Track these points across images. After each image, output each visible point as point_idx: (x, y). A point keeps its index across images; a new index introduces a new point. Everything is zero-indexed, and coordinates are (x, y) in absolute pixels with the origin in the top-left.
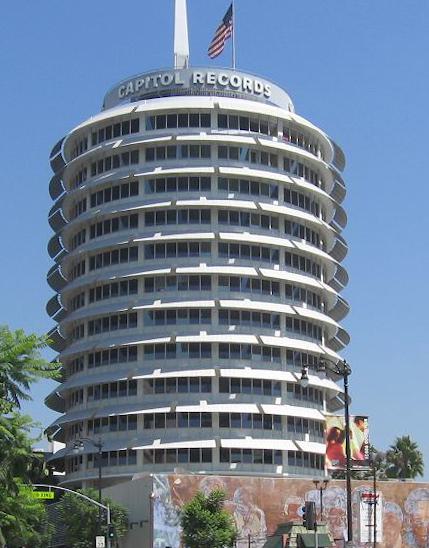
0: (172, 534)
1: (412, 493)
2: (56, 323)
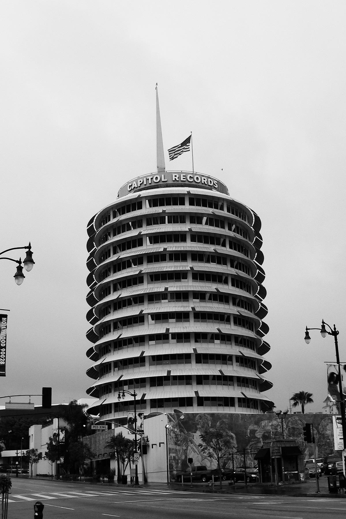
0: (179, 451)
1: (323, 421)
2: (91, 326)
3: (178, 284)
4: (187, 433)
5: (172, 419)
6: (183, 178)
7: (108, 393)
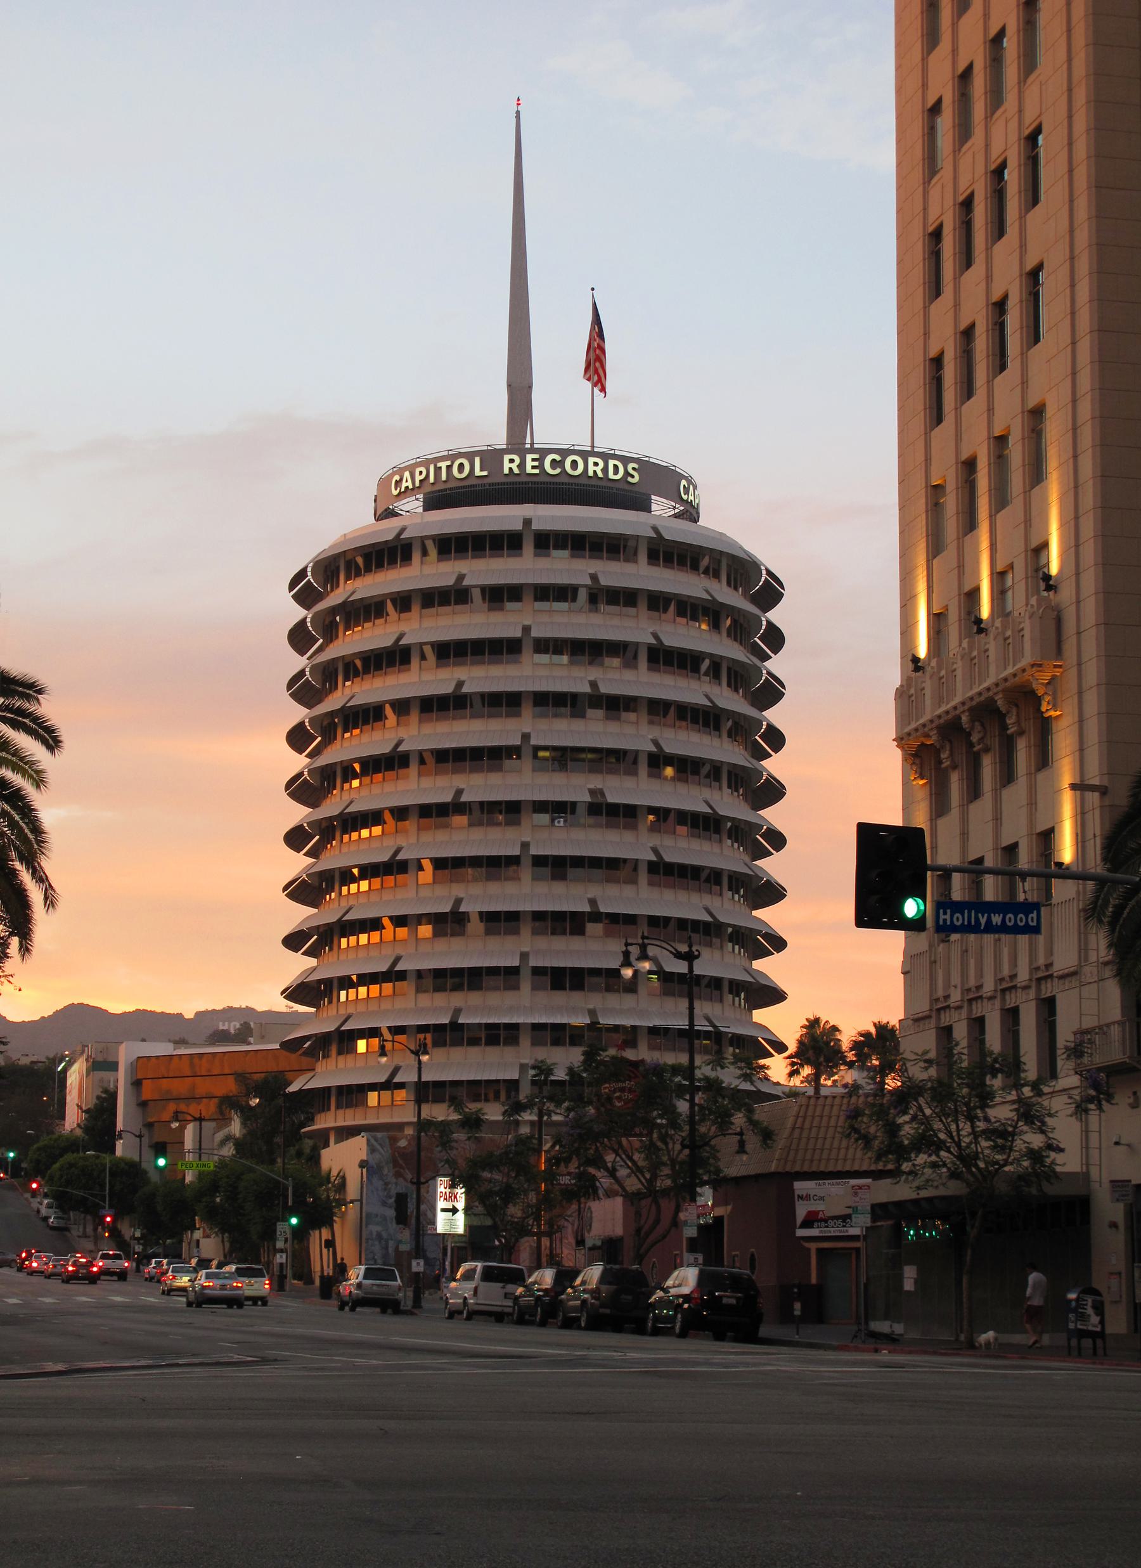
3: (494, 778)
5: (378, 1147)
6: (533, 467)
7: (343, 1054)
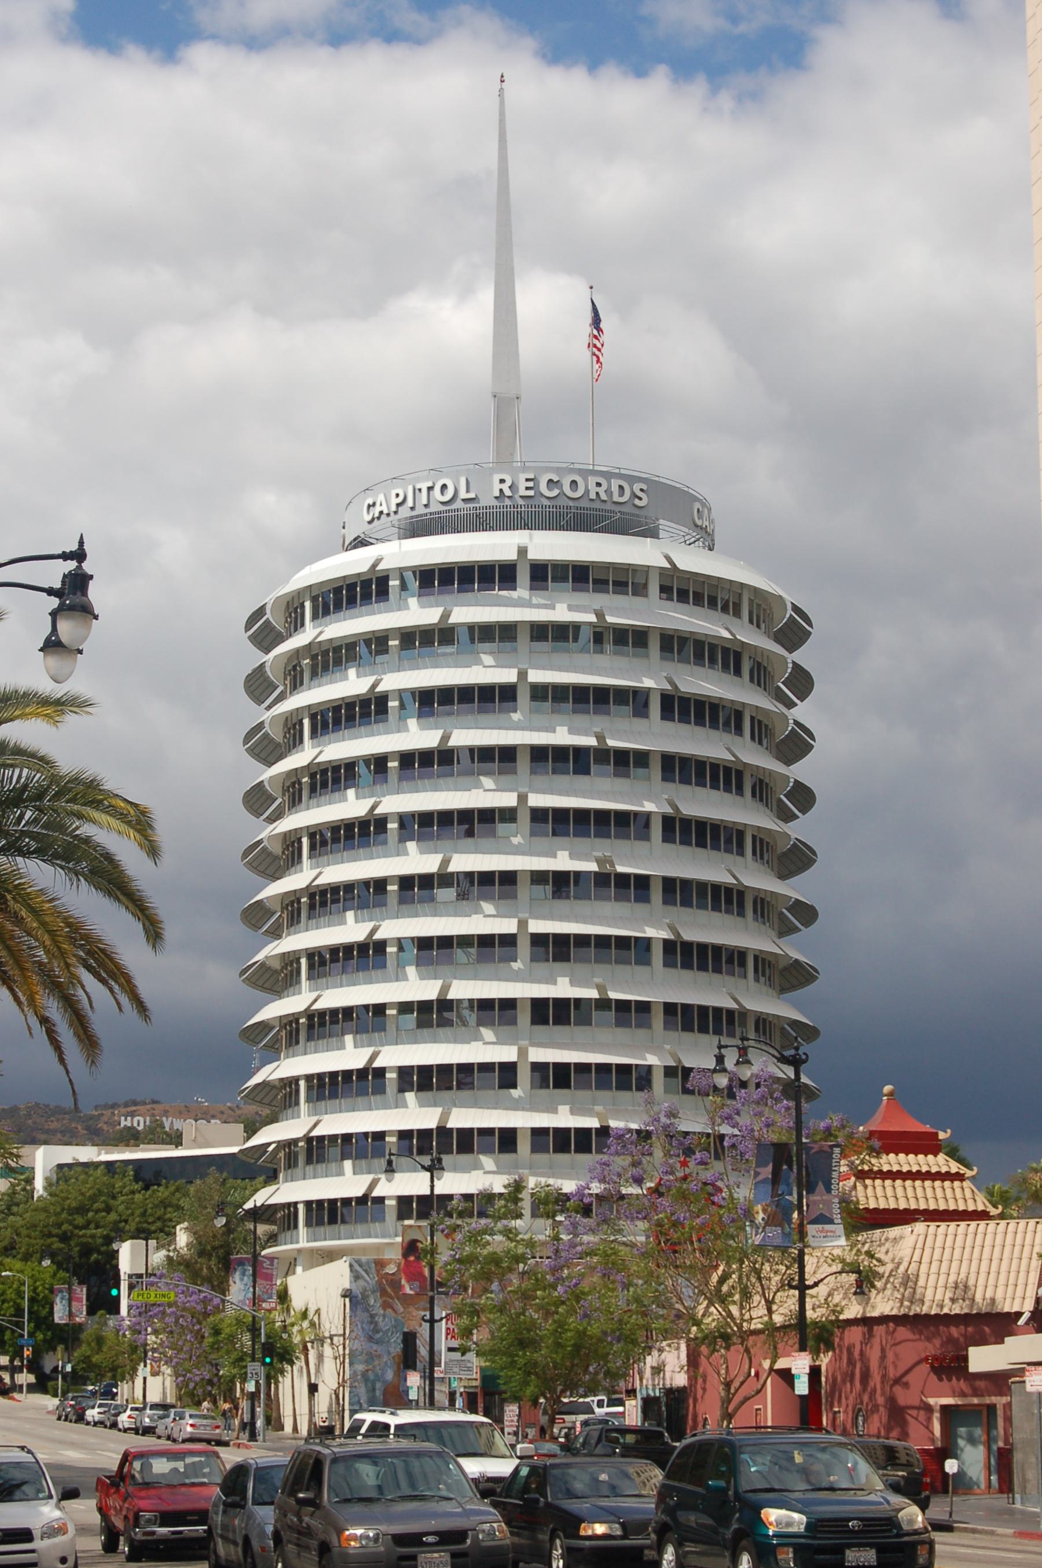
4: (402, 1310)
5: (363, 1273)
6: (527, 488)
